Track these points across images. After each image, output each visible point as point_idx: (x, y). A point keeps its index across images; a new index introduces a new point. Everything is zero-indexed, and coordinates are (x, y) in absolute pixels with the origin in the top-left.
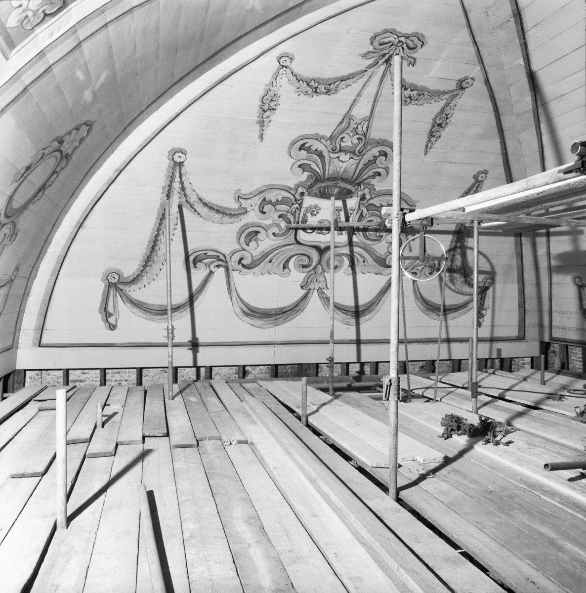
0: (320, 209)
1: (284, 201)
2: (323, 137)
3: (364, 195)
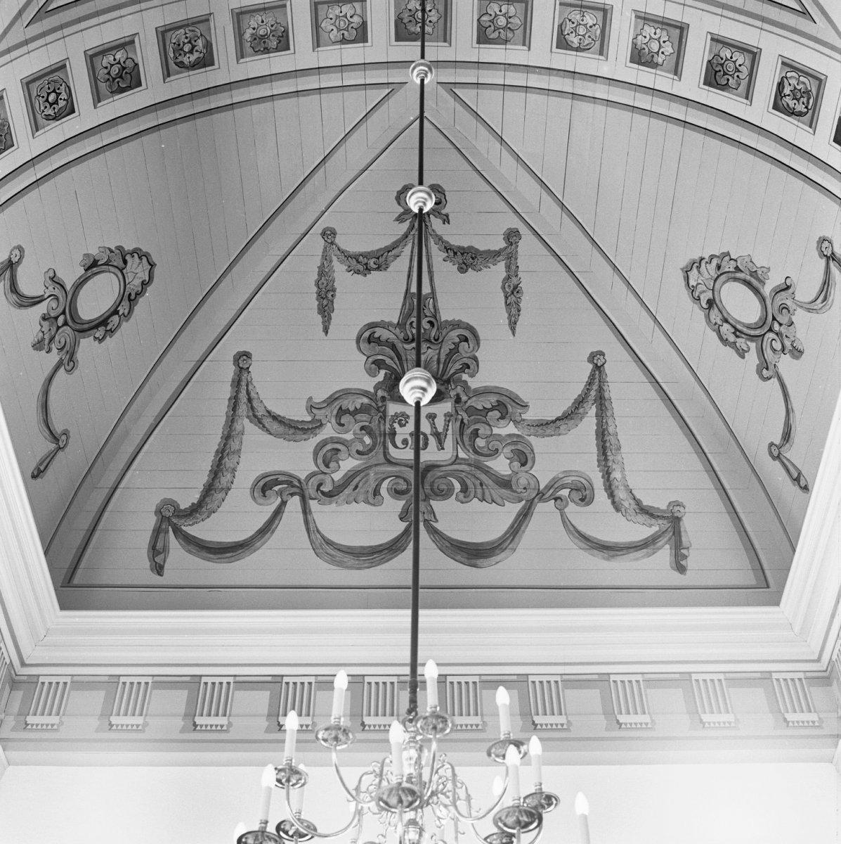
1: (364, 409)
2: (390, 324)
3: (458, 395)
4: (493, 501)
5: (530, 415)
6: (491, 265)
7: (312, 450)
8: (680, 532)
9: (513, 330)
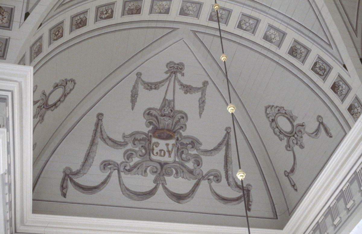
0: (159, 144)
2: (157, 109)
4: (187, 178)
5: (202, 148)
6: (196, 92)
7: (123, 153)
8: (249, 195)
9: (200, 116)
